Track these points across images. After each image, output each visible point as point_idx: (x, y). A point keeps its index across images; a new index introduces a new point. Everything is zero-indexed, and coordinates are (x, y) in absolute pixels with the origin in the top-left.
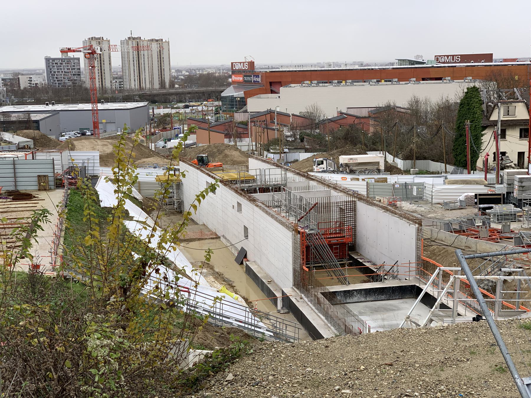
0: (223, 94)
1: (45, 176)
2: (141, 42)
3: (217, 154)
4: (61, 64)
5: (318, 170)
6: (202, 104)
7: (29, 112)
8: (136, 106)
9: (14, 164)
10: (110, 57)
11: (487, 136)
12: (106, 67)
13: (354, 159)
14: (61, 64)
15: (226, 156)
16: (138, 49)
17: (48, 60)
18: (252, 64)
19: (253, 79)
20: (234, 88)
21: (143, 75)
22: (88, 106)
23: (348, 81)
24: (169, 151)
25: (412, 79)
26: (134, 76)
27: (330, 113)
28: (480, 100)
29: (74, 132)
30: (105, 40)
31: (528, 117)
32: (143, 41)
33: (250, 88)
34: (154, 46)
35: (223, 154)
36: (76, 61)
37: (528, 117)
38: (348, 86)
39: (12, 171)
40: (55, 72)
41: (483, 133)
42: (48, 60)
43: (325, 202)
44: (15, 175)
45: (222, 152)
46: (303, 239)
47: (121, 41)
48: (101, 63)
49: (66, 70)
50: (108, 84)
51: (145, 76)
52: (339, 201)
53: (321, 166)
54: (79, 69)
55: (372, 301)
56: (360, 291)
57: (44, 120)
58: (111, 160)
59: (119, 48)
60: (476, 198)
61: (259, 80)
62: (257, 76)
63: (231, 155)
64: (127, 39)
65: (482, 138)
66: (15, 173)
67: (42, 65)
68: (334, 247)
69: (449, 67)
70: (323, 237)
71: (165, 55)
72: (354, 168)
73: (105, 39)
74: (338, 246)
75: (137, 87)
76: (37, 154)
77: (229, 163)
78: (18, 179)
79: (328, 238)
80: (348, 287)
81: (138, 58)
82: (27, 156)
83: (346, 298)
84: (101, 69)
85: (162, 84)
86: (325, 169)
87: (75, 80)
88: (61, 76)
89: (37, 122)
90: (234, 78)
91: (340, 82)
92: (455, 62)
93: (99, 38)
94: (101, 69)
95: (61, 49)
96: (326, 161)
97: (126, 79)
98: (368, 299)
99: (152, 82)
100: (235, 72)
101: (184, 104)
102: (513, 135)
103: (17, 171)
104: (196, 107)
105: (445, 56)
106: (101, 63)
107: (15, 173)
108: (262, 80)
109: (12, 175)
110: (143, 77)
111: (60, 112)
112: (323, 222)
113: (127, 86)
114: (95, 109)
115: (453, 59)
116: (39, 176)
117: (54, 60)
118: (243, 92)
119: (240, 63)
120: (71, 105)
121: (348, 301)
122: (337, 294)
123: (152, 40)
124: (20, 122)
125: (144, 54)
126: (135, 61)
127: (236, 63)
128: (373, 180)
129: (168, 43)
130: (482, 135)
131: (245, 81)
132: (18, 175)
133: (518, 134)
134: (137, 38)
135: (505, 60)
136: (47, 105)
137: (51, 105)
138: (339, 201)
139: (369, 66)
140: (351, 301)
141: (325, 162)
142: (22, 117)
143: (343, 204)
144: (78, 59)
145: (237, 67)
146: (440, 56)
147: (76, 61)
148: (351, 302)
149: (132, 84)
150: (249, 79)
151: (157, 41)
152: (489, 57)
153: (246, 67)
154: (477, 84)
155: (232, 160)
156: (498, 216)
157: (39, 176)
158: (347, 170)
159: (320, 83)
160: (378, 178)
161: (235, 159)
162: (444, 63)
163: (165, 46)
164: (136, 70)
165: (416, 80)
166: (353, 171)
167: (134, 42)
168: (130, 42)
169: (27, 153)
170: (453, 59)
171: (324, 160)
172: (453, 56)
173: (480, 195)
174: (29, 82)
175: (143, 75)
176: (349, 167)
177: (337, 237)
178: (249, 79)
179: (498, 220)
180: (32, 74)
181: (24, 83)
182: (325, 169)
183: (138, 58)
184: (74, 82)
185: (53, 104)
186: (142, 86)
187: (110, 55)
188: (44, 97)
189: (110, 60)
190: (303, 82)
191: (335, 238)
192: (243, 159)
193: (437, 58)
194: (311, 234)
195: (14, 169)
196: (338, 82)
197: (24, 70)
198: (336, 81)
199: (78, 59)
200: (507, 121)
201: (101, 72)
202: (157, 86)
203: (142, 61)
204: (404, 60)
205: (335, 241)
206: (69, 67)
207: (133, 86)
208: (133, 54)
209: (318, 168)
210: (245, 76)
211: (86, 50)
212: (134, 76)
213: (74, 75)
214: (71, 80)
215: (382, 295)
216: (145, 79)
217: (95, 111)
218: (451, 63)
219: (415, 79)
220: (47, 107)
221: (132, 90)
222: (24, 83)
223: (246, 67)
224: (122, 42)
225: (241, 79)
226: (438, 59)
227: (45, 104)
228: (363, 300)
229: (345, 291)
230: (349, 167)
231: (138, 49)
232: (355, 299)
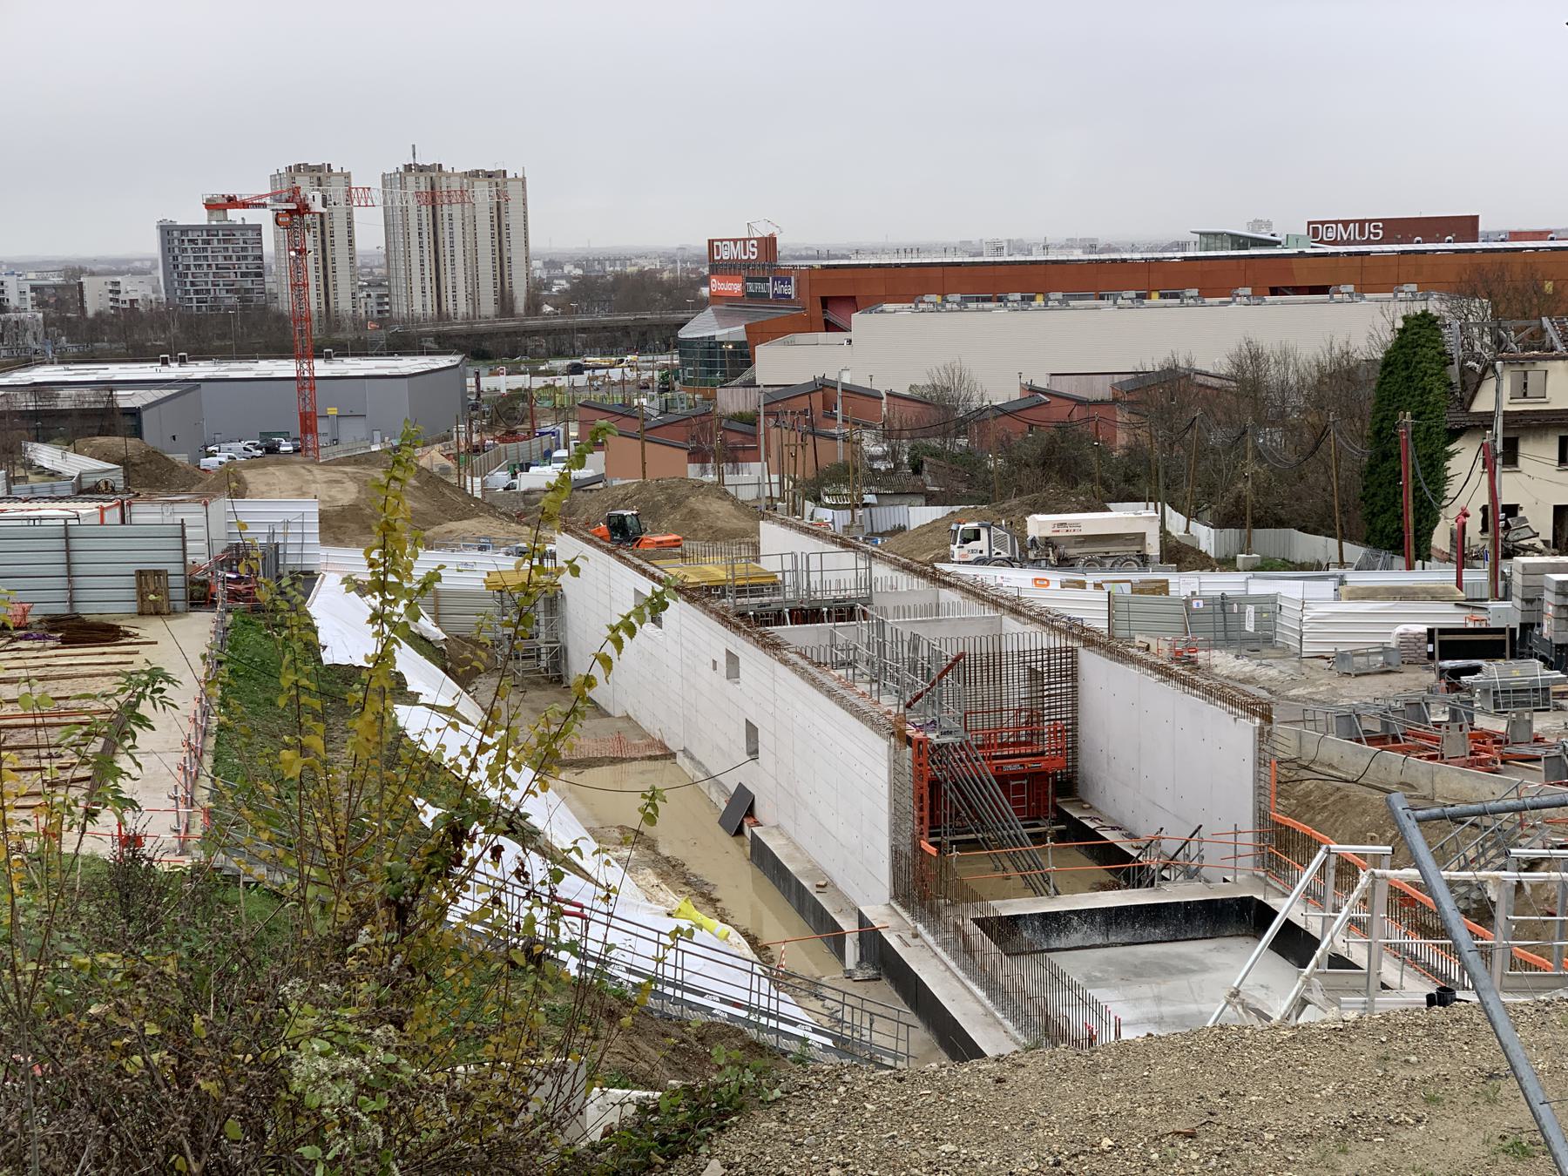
0: (685, 333)
1: (157, 573)
2: (443, 179)
3: (667, 509)
4: (207, 242)
5: (964, 556)
6: (622, 361)
7: (111, 385)
8: (427, 368)
9: (67, 538)
10: (350, 224)
11: (1464, 460)
13: (1071, 525)
14: (207, 242)
15: (693, 515)
16: (433, 198)
17: (167, 231)
18: (768, 244)
19: (773, 288)
20: (717, 313)
21: (449, 275)
22: (286, 368)
23: (1052, 295)
24: (524, 501)
25: (1241, 291)
26: (423, 279)
27: (1000, 389)
28: (1443, 353)
29: (244, 444)
30: (338, 174)
32: (448, 176)
33: (763, 315)
35: (685, 511)
36: (250, 234)
38: (1052, 309)
39: (62, 557)
40: (188, 267)
41: (1451, 448)
42: (167, 231)
43: (984, 651)
44: (69, 569)
45: (680, 503)
46: (921, 760)
47: (384, 175)
48: (323, 241)
49: (221, 261)
50: (344, 303)
51: (456, 278)
52: (1027, 648)
53: (973, 545)
54: (261, 258)
55: (1124, 945)
56: (1088, 915)
57: (155, 409)
58: (353, 526)
59: (377, 196)
60: (1431, 640)
61: (791, 290)
63: (709, 512)
64: (401, 170)
65: (1447, 464)
66: (69, 563)
67: (150, 247)
68: (1012, 783)
69: (1349, 254)
70: (980, 756)
71: (513, 218)
72: (1072, 552)
73: (336, 169)
74: (1025, 782)
75: (429, 311)
76: (135, 508)
77: (701, 535)
78: (80, 582)
79: (996, 758)
80: (1055, 901)
81: (435, 225)
82: (106, 513)
83: (1048, 937)
84: (324, 259)
85: (505, 301)
86: (986, 554)
87: (247, 291)
88: (206, 280)
89: (134, 413)
90: (717, 285)
92: (1369, 242)
93: (319, 168)
94: (324, 259)
95: (208, 200)
96: (989, 529)
97: (399, 291)
98: (1113, 939)
99: (474, 299)
100: (720, 268)
101: (568, 362)
102: (1539, 454)
103: (76, 557)
104: (603, 372)
105: (1336, 222)
106: (323, 241)
107: (69, 563)
109: (62, 570)
110: (447, 281)
111: (202, 384)
112: (980, 709)
113: (400, 309)
114: (307, 375)
115: (1362, 233)
116: (140, 573)
117: (185, 230)
118: (743, 327)
119: (735, 241)
121: (1055, 944)
122: (1020, 923)
123: (475, 174)
124: (85, 414)
125: (450, 215)
126: (425, 235)
127: (722, 241)
128: (1127, 588)
129: (523, 181)
130: (1449, 456)
132: (78, 569)
133: (1554, 454)
135: (1515, 236)
136: (165, 362)
137: (176, 365)
138: (1027, 648)
140: (1063, 943)
141: (984, 534)
142: (90, 399)
143: (1039, 657)
144: (258, 229)
146: (1323, 223)
147: (250, 234)
148: (1062, 946)
149: (416, 303)
150: (760, 287)
151: (490, 175)
152: (1467, 226)
153: (753, 254)
154: (1435, 306)
155: (710, 527)
156: (1496, 693)
157: (140, 571)
158: (1051, 557)
159: (971, 300)
160: (1141, 582)
161: (719, 524)
162: (1334, 243)
163: (513, 191)
164: (426, 263)
165: (1254, 294)
166: (1066, 560)
167: (422, 179)
168: (410, 179)
169: (105, 505)
170: (1362, 233)
171: (983, 526)
172: (1362, 223)
173: (1443, 631)
174: (111, 296)
175: (449, 275)
176: (1055, 548)
177: (1020, 756)
178: (760, 287)
179: (1496, 705)
180: (121, 273)
181: (96, 299)
182: (986, 554)
183: (435, 225)
184: (244, 295)
185: (182, 361)
186: (444, 309)
187: (350, 215)
189: (350, 233)
190: (919, 298)
191: (1014, 756)
192: (742, 525)
193: (1314, 229)
194: (946, 746)
195: (68, 551)
196: (1023, 299)
197: (95, 261)
198: (1018, 296)
199: (258, 229)
200: (1521, 413)
201: (325, 268)
202: (488, 307)
203: (444, 235)
204: (1216, 234)
205: (1016, 767)
206: (230, 253)
207: (418, 308)
208: (417, 214)
209: (964, 551)
210: (749, 279)
211: (280, 201)
212: (423, 279)
213: (244, 275)
214: (237, 291)
215: (1155, 927)
216: (454, 287)
217: (305, 383)
218: (1355, 243)
219: (1248, 291)
220: (165, 368)
221: (413, 320)
222: (96, 299)
223: (753, 254)
224: (386, 180)
225: (735, 288)
226: (1316, 230)
227: (157, 361)
228: (1099, 940)
229: (1045, 916)
230: (1055, 548)
231: (433, 199)
232: (1076, 939)
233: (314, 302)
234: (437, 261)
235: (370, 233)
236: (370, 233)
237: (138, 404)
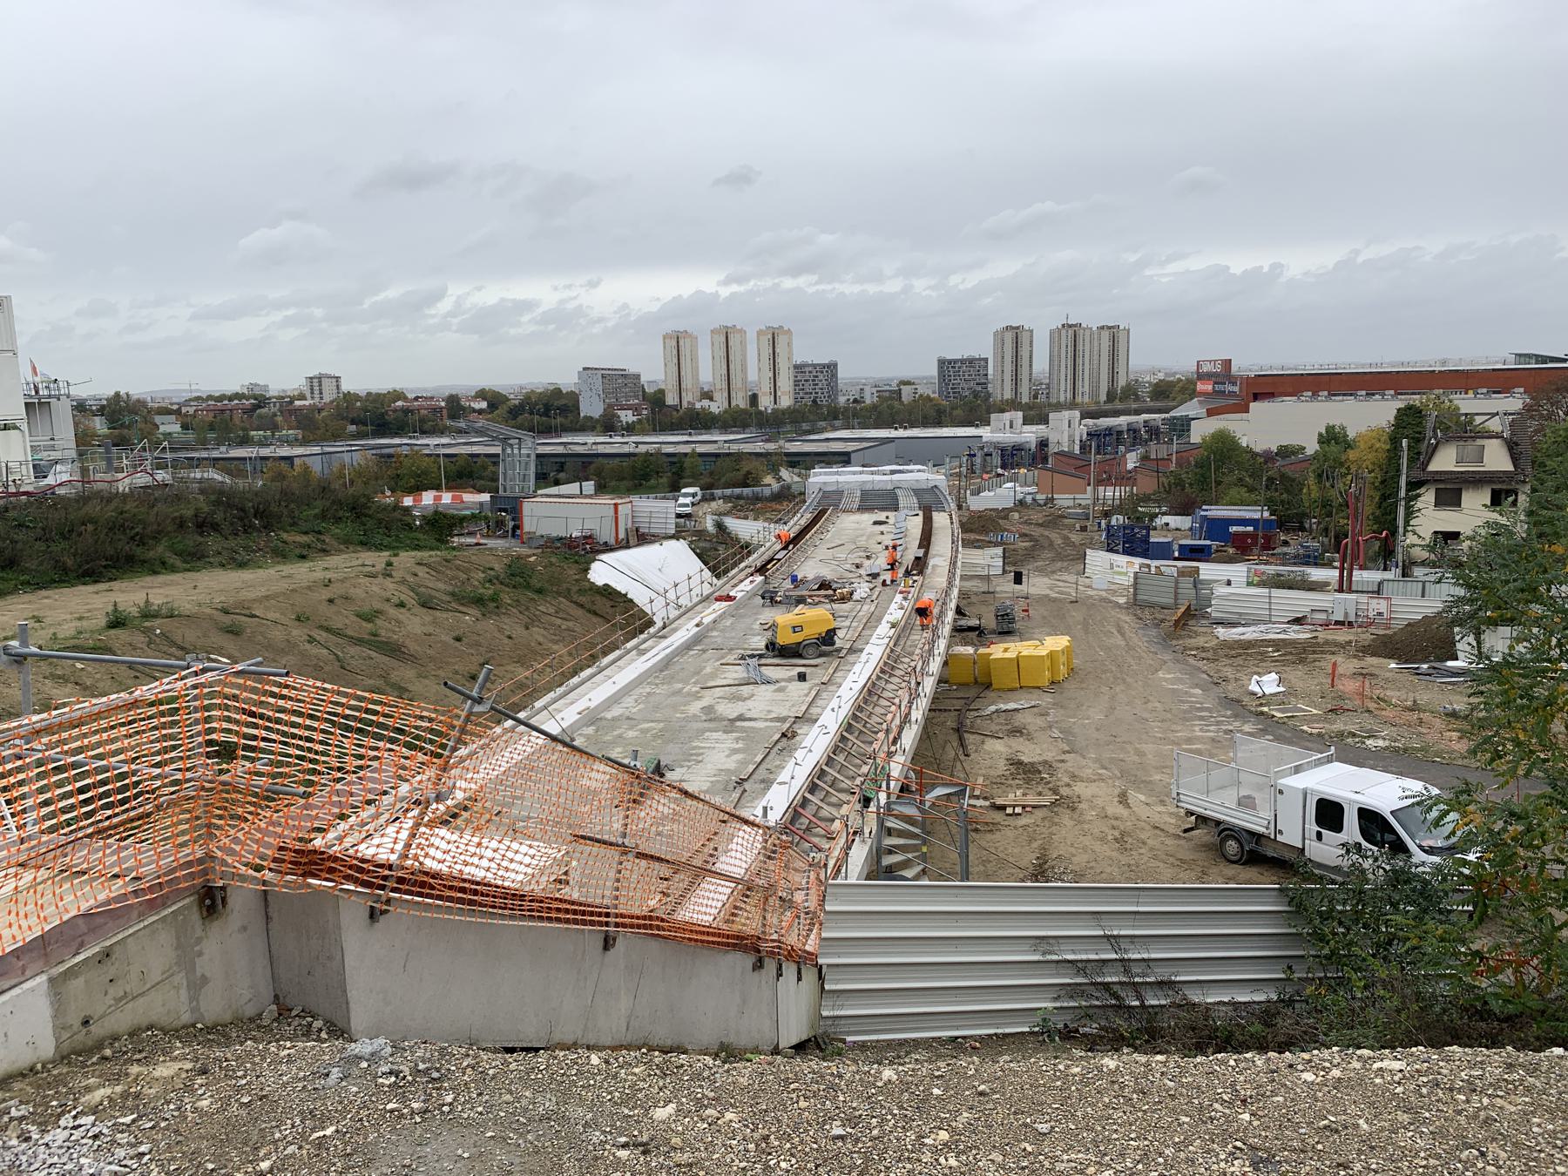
10: (1031, 357)
17: (943, 364)
23: (1387, 392)
25: (1516, 390)
31: (1511, 468)
32: (1084, 329)
33: (1221, 402)
34: (1106, 335)
37: (1511, 468)
38: (1387, 400)
42: (943, 364)
49: (966, 377)
51: (1084, 387)
54: (986, 375)
61: (1236, 389)
62: (1234, 384)
64: (1060, 327)
67: (933, 371)
73: (1026, 327)
90: (1200, 387)
91: (1315, 394)
93: (1018, 328)
97: (1054, 391)
99: (1095, 392)
100: (1201, 376)
108: (1240, 389)
117: (950, 362)
119: (1210, 361)
120: (931, 430)
123: (1102, 328)
131: (1215, 392)
134: (1075, 325)
136: (896, 429)
139: (1289, 369)
145: (1206, 368)
147: (982, 363)
150: (1221, 387)
154: (1416, 400)
163: (1122, 337)
168: (1063, 332)
169: (619, 501)
178: (1221, 387)
185: (906, 428)
189: (1031, 361)
198: (1364, 393)
200: (1462, 472)
202: (1103, 397)
204: (1525, 355)
207: (1062, 399)
210: (1215, 383)
225: (1209, 388)
234: (1074, 374)
235: (1041, 365)
236: (1041, 365)
237: (849, 449)
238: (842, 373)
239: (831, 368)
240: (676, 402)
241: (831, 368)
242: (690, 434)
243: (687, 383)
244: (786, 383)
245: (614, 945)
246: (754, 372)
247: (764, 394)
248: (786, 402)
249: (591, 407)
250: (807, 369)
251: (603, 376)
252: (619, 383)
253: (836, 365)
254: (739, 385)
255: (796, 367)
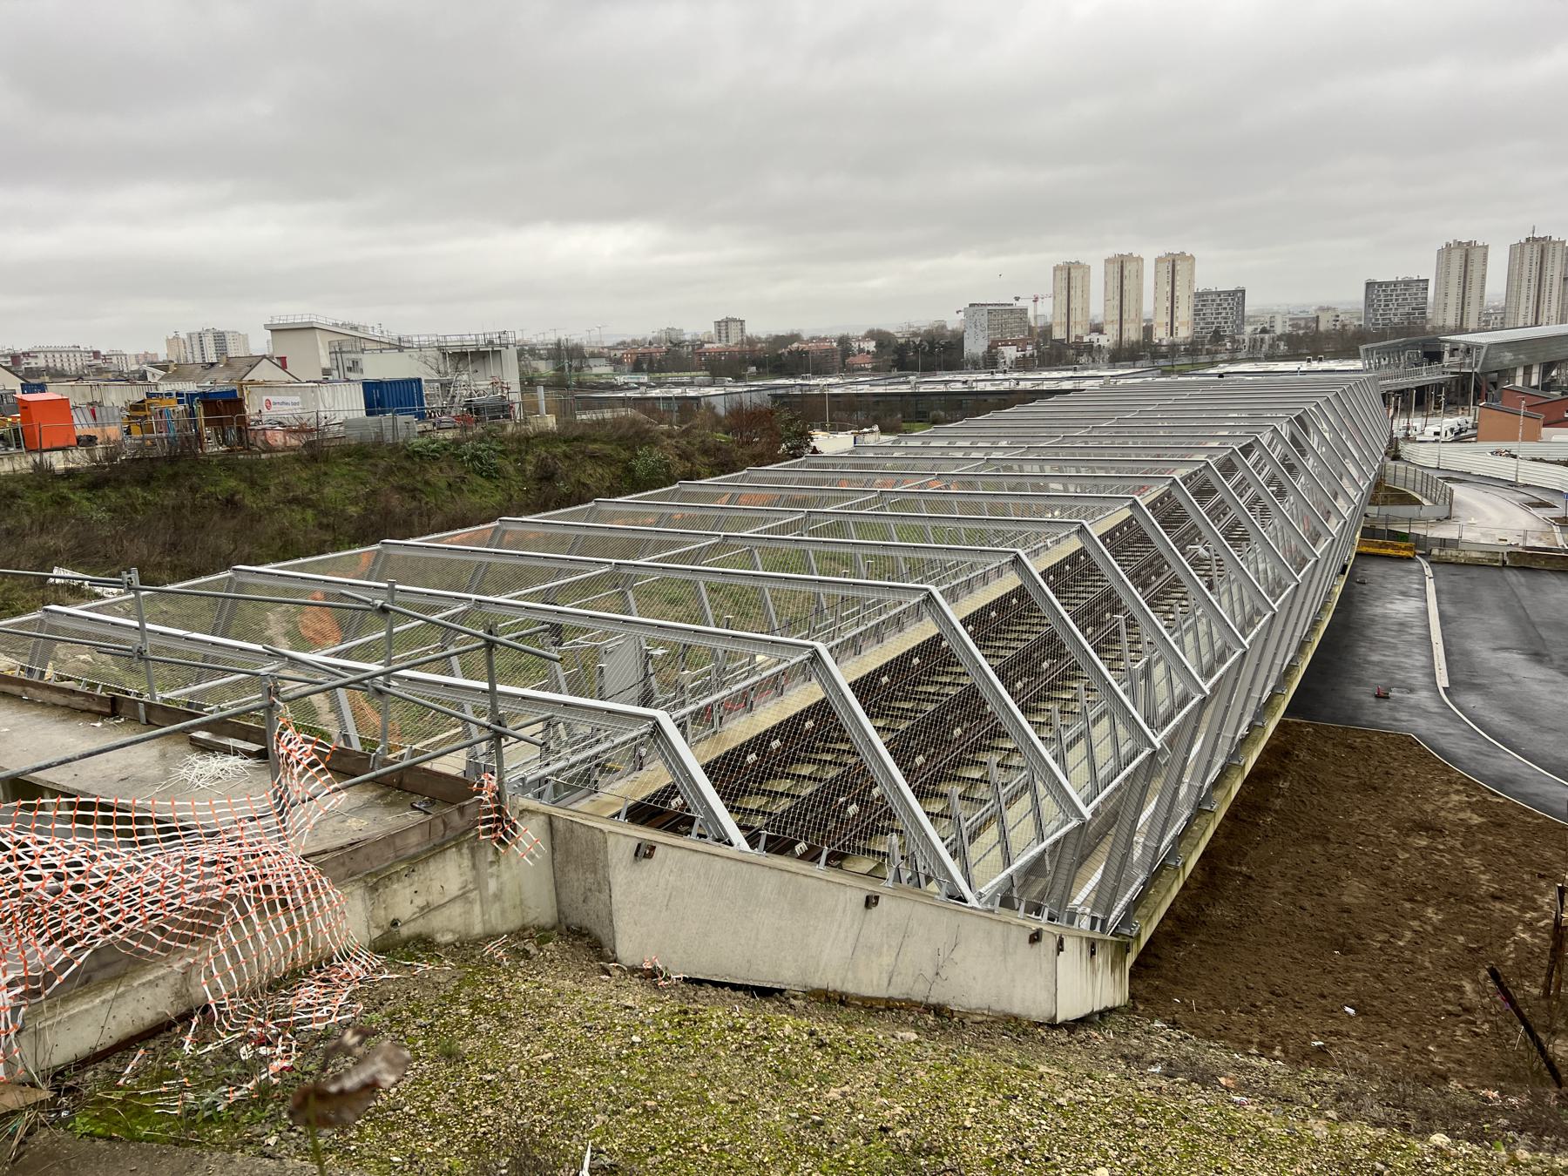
10: (1484, 277)
12: (1473, 294)
17: (1370, 285)
32: (1555, 243)
42: (1370, 285)
67: (1359, 296)
93: (1469, 244)
117: (1380, 284)
120: (1346, 362)
136: (1309, 361)
168: (1528, 248)
185: (1320, 360)
188: (1330, 348)
208: (1529, 271)
233: (59, 365)
235: (1495, 285)
236: (1495, 285)
238: (1252, 305)
239: (1238, 295)
240: (1064, 336)
241: (1238, 295)
242: (1075, 369)
243: (1077, 316)
244: (1184, 313)
245: (876, 904)
246: (1149, 302)
247: (1159, 325)
248: (1184, 333)
249: (975, 346)
250: (1210, 298)
251: (989, 312)
252: (1004, 318)
253: (1243, 292)
254: (1133, 315)
255: (1198, 295)
